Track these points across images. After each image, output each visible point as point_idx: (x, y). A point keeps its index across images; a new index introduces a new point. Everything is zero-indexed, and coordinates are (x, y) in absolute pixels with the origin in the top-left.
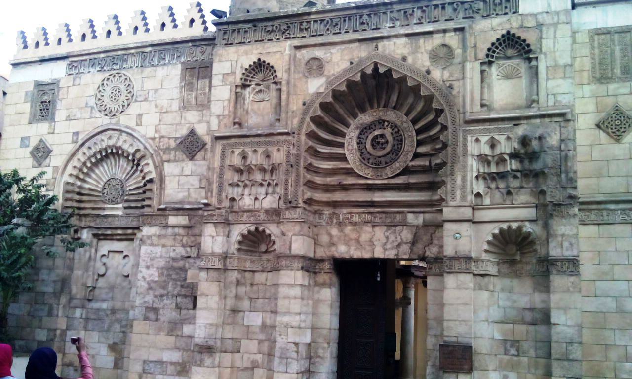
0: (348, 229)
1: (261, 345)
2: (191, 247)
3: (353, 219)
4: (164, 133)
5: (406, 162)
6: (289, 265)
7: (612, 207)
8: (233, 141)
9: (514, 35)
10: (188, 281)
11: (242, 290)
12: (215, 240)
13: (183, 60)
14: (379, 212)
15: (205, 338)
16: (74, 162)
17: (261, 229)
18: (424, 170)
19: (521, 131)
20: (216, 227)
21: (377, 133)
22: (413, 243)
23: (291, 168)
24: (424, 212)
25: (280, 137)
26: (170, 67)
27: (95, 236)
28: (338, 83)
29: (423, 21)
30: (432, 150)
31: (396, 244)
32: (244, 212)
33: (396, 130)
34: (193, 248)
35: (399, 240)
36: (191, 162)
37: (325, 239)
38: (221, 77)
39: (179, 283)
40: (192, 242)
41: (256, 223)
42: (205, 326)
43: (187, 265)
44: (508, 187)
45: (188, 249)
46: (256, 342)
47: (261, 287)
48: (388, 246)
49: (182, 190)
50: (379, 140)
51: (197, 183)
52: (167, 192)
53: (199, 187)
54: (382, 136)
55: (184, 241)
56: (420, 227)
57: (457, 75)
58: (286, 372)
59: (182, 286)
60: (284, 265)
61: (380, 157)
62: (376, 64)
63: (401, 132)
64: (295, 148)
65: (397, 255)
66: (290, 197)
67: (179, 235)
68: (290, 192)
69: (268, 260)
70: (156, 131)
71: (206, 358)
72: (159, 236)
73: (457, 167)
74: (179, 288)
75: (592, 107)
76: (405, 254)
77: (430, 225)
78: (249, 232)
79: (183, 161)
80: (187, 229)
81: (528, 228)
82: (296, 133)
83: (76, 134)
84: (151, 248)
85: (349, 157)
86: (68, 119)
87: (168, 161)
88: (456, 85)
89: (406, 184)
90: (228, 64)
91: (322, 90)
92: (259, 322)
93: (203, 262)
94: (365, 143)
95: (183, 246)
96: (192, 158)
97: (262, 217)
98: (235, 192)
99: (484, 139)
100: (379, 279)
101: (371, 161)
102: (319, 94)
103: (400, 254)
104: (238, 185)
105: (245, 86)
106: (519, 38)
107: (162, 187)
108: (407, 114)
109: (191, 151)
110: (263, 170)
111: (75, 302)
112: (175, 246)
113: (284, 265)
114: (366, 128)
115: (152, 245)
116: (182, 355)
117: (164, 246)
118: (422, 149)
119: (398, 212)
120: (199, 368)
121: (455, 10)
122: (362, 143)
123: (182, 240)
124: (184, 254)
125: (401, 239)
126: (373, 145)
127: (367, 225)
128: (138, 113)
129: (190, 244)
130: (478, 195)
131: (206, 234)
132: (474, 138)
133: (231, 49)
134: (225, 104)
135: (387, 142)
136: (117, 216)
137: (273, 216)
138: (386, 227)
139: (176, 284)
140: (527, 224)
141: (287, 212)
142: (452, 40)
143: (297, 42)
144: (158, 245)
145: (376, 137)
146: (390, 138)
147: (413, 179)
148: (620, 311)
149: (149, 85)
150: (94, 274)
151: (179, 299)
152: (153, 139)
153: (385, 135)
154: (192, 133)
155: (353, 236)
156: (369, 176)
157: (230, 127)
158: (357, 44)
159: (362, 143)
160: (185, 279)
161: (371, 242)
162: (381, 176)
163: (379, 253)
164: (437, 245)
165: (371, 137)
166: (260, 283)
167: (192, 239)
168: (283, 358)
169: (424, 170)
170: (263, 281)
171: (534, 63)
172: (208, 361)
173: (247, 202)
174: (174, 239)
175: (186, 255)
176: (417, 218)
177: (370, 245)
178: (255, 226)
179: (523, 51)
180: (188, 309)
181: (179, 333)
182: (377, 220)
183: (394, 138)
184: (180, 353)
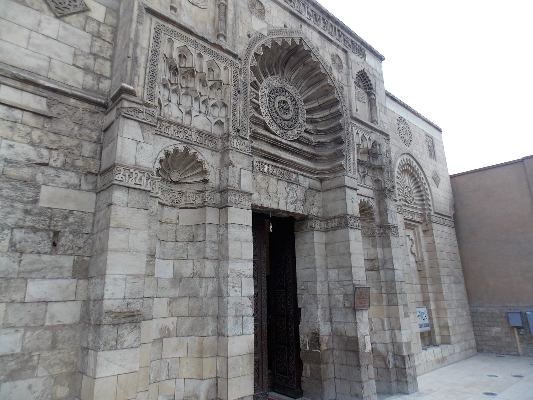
1: (174, 304)
2: (49, 149)
3: (263, 169)
5: (300, 132)
6: (238, 202)
8: (170, 26)
9: (365, 74)
10: (41, 204)
12: (142, 148)
14: (282, 168)
15: (124, 299)
17: (192, 151)
18: (308, 143)
20: (142, 128)
22: (305, 201)
23: (239, 95)
24: (309, 178)
25: (226, 55)
28: (277, 37)
29: (325, 29)
30: (313, 130)
31: (294, 200)
32: (170, 123)
34: (53, 152)
35: (296, 198)
36: (57, 21)
39: (20, 206)
40: (53, 142)
41: (186, 143)
42: (125, 279)
43: (40, 178)
44: (364, 172)
45: (45, 152)
46: (165, 301)
47: (170, 227)
48: (289, 201)
49: (37, 55)
53: (71, 64)
54: (285, 102)
56: (307, 189)
57: (345, 82)
58: (242, 334)
59: (27, 212)
60: (233, 201)
61: (284, 120)
62: (301, 40)
64: (243, 75)
65: (295, 209)
66: (238, 125)
68: (238, 119)
69: (181, 193)
71: (126, 332)
73: (351, 147)
74: (19, 214)
77: (313, 189)
78: (176, 151)
79: (40, 11)
80: (42, 119)
82: (243, 59)
85: (263, 110)
88: (345, 88)
89: (301, 150)
91: (265, 33)
92: (169, 274)
93: (120, 176)
95: (32, 144)
96: (60, 17)
97: (193, 137)
98: (162, 93)
100: (271, 230)
101: (278, 120)
106: (367, 77)
108: (300, 93)
109: (60, 6)
110: (203, 82)
113: (233, 201)
116: (23, 337)
118: (309, 127)
119: (294, 173)
120: (113, 352)
121: (340, 36)
127: (273, 178)
129: (46, 143)
132: (356, 131)
137: (207, 141)
138: (286, 183)
139: (13, 207)
140: (370, 200)
141: (235, 141)
142: (342, 55)
146: (291, 107)
147: (305, 149)
151: (18, 234)
153: (287, 103)
155: (263, 185)
157: (167, 8)
158: (288, 14)
160: (36, 201)
163: (283, 206)
166: (169, 221)
167: (53, 137)
168: (239, 316)
169: (308, 143)
170: (174, 220)
171: (373, 97)
172: (129, 337)
173: (173, 112)
174: (11, 127)
175: (39, 161)
177: (275, 197)
178: (185, 145)
179: (367, 87)
180: (39, 253)
181: (17, 297)
184: (19, 335)
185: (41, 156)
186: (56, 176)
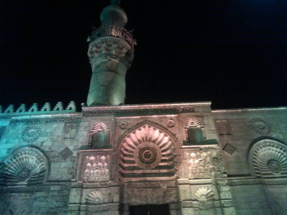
2: (60, 202)
4: (53, 150)
13: (65, 121)
21: (147, 151)
26: (59, 124)
31: (157, 197)
33: (154, 150)
37: (125, 196)
38: (84, 127)
43: (58, 211)
45: (59, 203)
48: (153, 198)
50: (147, 154)
51: (66, 171)
52: (52, 175)
54: (148, 152)
55: (57, 199)
63: (156, 151)
65: (157, 202)
67: (55, 196)
70: (49, 149)
72: (45, 197)
76: (161, 201)
83: (9, 149)
84: (40, 203)
87: (54, 162)
90: (88, 123)
94: (142, 155)
95: (57, 201)
103: (159, 201)
107: (49, 174)
112: (52, 202)
114: (142, 149)
115: (40, 201)
122: (140, 155)
123: (56, 199)
124: (57, 205)
125: (159, 195)
126: (145, 156)
128: (42, 140)
131: (72, 195)
133: (89, 118)
134: (85, 138)
135: (150, 155)
144: (43, 201)
145: (146, 153)
149: (48, 130)
154: (67, 149)
156: (144, 168)
159: (140, 155)
161: (146, 197)
162: (149, 168)
163: (150, 202)
164: (173, 197)
165: (144, 152)
167: (62, 198)
176: (164, 185)
182: (148, 187)
183: (153, 153)
185: (58, 204)
186: (62, 209)
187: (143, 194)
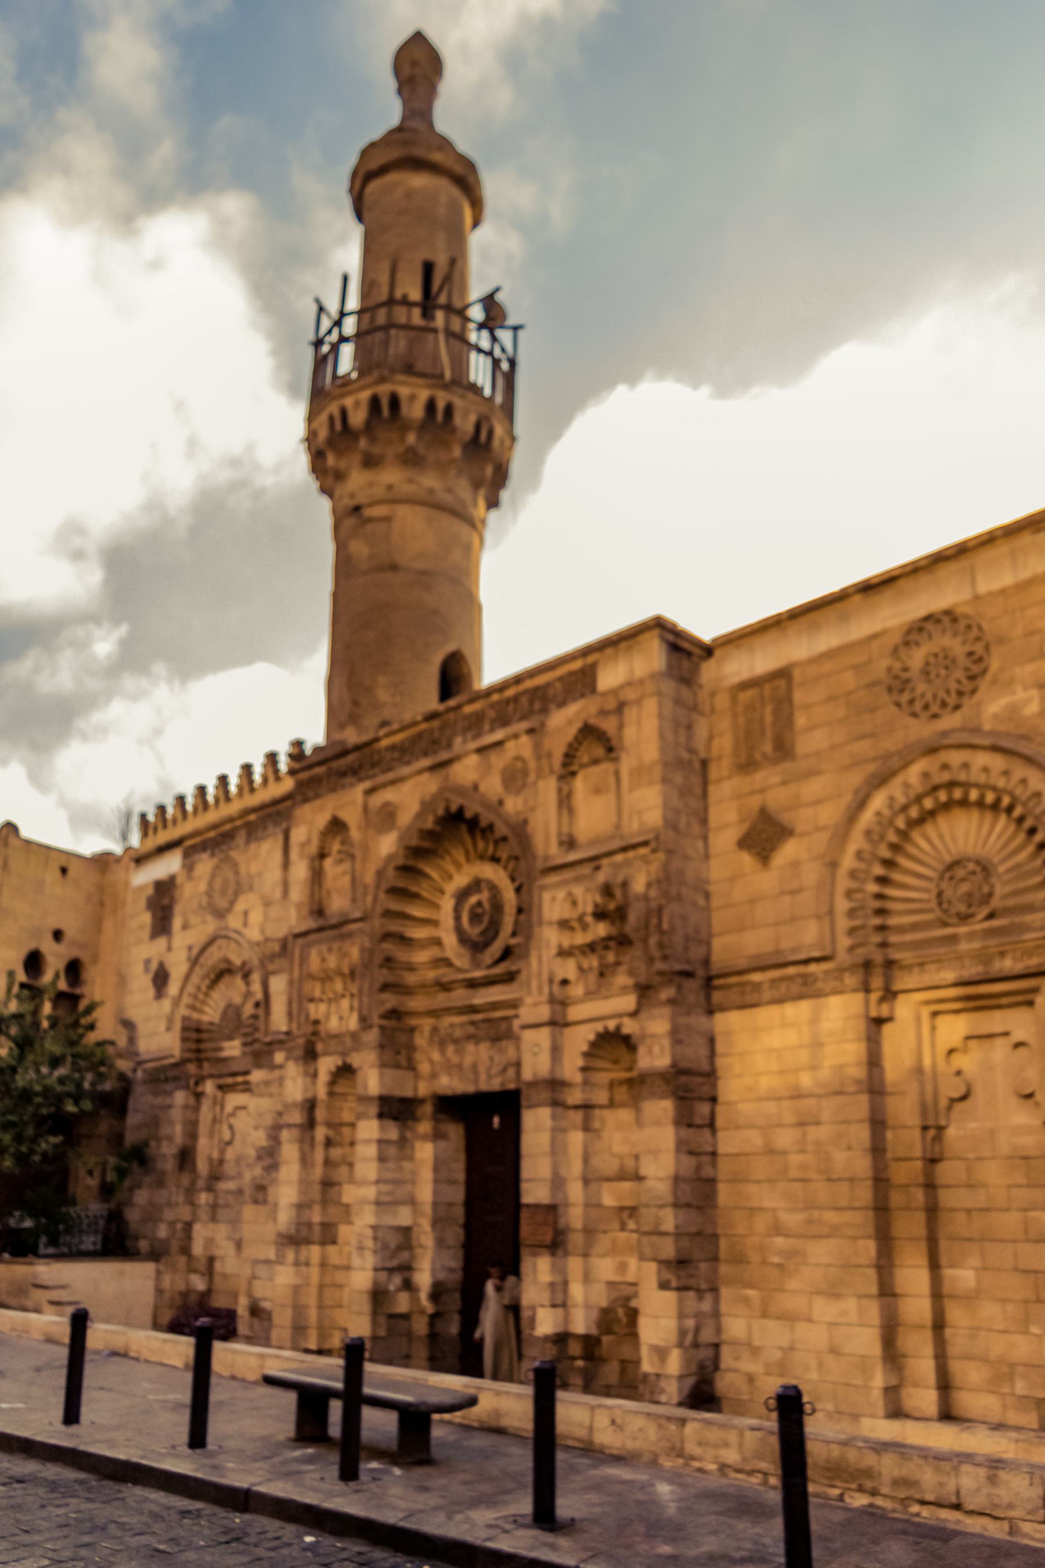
0: (451, 1049)
7: (756, 977)
11: (336, 1153)
16: (190, 989)
19: (601, 877)
27: (220, 1087)
37: (424, 1068)
54: (479, 904)
65: (502, 1084)
70: (262, 931)
75: (732, 816)
81: (629, 1027)
86: (185, 927)
99: (561, 894)
102: (390, 857)
104: (321, 1000)
105: (322, 855)
111: (201, 1183)
117: (271, 1095)
130: (565, 982)
136: (232, 1058)
143: (367, 784)
148: (770, 1151)
150: (220, 1142)
152: (258, 944)
163: (484, 1086)
182: (481, 1033)
187: (468, 1061)
